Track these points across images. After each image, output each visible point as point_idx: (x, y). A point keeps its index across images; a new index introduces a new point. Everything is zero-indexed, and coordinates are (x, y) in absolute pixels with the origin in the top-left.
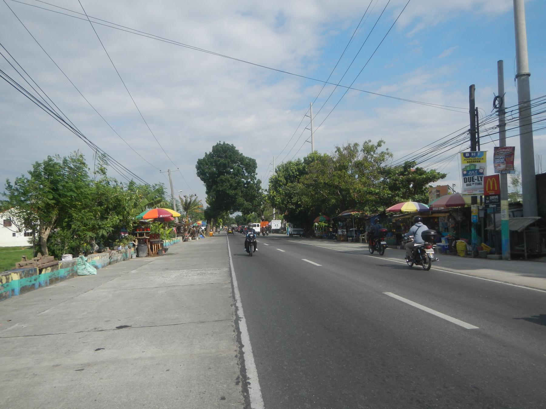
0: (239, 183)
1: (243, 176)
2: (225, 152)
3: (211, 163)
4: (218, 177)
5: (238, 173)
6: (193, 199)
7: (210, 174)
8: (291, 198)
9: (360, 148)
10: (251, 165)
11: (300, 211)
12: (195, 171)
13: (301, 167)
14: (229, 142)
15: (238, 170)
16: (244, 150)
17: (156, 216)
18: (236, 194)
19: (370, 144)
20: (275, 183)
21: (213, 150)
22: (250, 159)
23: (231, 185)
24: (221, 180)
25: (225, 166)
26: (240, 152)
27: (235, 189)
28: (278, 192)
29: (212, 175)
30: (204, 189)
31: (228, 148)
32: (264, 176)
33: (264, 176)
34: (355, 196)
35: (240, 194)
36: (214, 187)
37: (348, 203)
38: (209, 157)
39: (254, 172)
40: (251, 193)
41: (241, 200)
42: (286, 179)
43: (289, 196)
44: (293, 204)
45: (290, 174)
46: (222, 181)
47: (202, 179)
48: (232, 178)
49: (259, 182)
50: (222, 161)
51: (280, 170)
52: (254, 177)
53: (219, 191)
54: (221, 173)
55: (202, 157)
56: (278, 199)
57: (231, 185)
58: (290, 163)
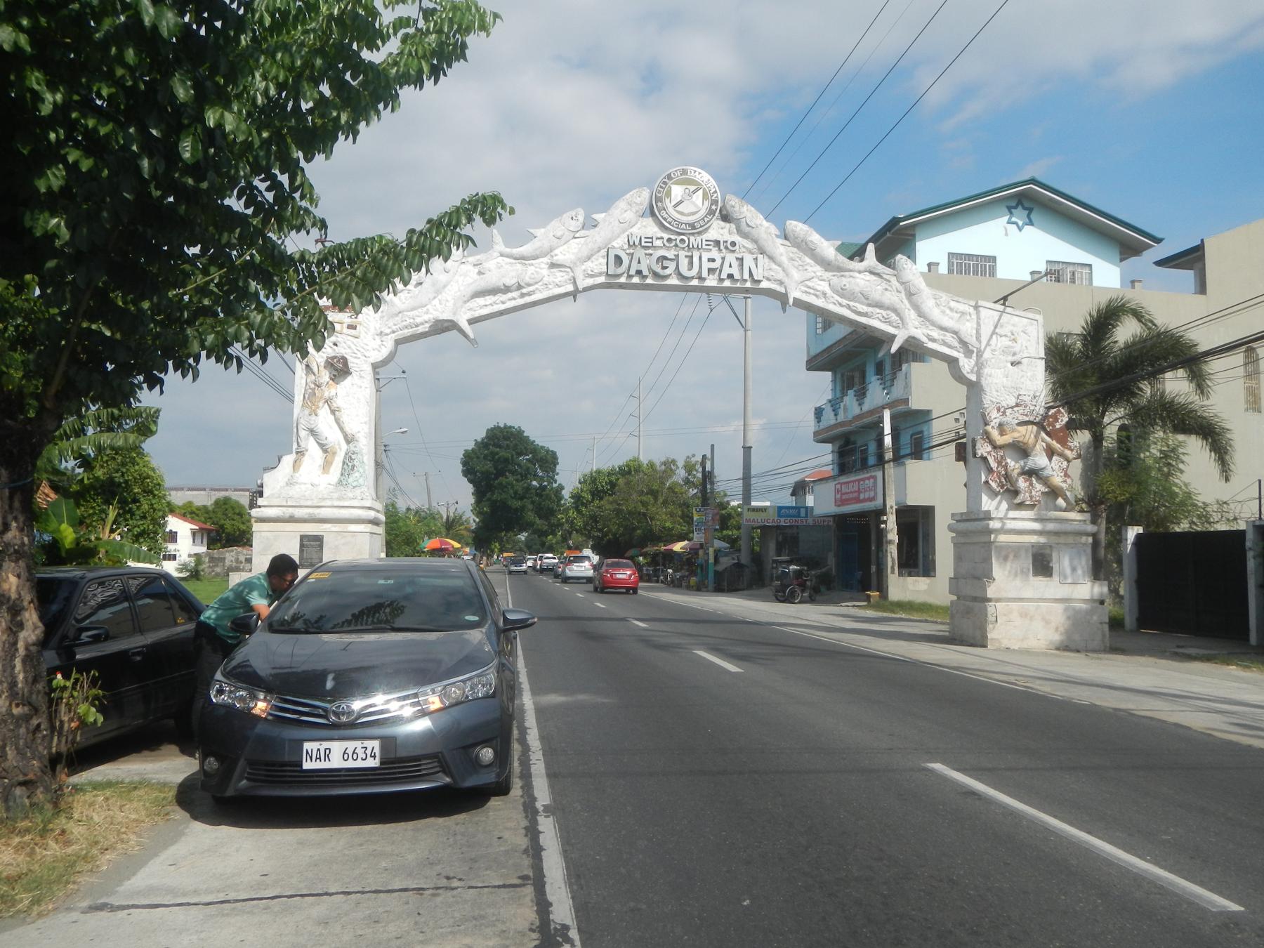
0: (528, 488)
1: (535, 476)
2: (506, 438)
3: (485, 457)
4: (497, 478)
5: (526, 474)
6: (452, 510)
7: (482, 473)
8: (596, 522)
9: (681, 463)
10: (548, 461)
11: (609, 541)
12: (460, 467)
13: (613, 478)
14: (514, 423)
15: (528, 469)
16: (538, 434)
17: (437, 545)
18: (523, 508)
19: (693, 460)
20: (577, 497)
21: (487, 437)
22: (547, 451)
23: (516, 493)
24: (501, 484)
25: (506, 460)
26: (532, 439)
27: (521, 498)
28: (579, 512)
29: (486, 475)
30: (472, 500)
31: (512, 433)
32: (568, 479)
33: (568, 479)
34: (656, 529)
35: (530, 507)
36: (488, 495)
37: (653, 537)
38: (483, 445)
39: (554, 471)
40: (546, 502)
41: (531, 516)
42: (593, 494)
43: (594, 518)
44: (600, 530)
45: (600, 487)
46: (503, 487)
47: (470, 481)
48: (517, 480)
49: (561, 488)
50: (503, 453)
51: (585, 482)
52: (553, 478)
53: (496, 501)
54: (500, 473)
55: (470, 446)
56: (579, 523)
57: (516, 493)
58: (598, 472)
